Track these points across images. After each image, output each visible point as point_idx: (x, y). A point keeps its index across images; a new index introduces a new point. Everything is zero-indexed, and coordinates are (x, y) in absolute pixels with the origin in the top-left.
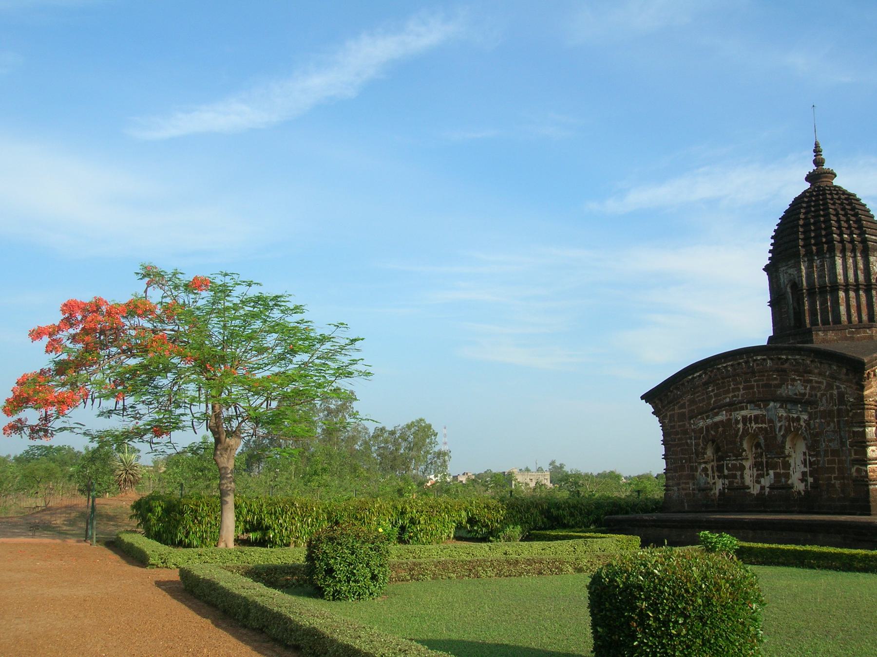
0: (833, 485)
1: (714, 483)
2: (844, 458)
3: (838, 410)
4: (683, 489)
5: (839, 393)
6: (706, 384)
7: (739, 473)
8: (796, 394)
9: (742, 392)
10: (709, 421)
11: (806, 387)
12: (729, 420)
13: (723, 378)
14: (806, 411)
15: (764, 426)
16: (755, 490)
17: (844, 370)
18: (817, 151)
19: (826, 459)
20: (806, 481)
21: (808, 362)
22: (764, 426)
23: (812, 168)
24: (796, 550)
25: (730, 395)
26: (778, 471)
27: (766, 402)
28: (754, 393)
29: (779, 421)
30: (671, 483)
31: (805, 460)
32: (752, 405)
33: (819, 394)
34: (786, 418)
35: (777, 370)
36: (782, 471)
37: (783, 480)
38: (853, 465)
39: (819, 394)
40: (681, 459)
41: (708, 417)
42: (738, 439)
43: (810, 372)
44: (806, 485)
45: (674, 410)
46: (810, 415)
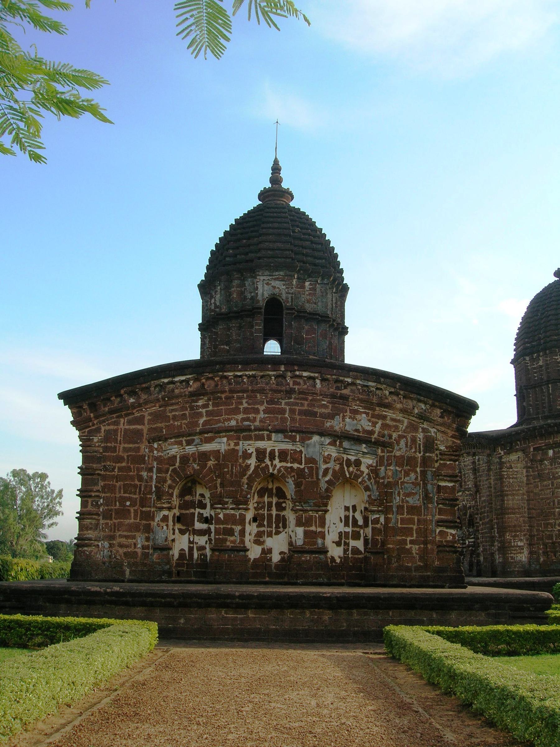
0: (409, 551)
1: (173, 540)
3: (424, 458)
4: (121, 546)
5: (426, 437)
6: (196, 395)
7: (237, 528)
8: (357, 430)
9: (262, 415)
10: (191, 449)
11: (374, 424)
12: (232, 454)
13: (232, 391)
15: (296, 466)
16: (255, 552)
17: (438, 412)
18: (276, 169)
19: (399, 517)
20: (347, 544)
21: (387, 393)
22: (296, 466)
23: (268, 185)
25: (240, 417)
26: (313, 528)
27: (306, 434)
28: (284, 420)
29: (325, 462)
30: (90, 534)
31: (347, 518)
32: (280, 436)
33: (395, 435)
34: (337, 460)
35: (333, 396)
36: (319, 529)
37: (320, 541)
39: (395, 435)
40: (122, 500)
41: (189, 443)
42: (245, 480)
43: (388, 406)
44: (345, 551)
45: (117, 423)
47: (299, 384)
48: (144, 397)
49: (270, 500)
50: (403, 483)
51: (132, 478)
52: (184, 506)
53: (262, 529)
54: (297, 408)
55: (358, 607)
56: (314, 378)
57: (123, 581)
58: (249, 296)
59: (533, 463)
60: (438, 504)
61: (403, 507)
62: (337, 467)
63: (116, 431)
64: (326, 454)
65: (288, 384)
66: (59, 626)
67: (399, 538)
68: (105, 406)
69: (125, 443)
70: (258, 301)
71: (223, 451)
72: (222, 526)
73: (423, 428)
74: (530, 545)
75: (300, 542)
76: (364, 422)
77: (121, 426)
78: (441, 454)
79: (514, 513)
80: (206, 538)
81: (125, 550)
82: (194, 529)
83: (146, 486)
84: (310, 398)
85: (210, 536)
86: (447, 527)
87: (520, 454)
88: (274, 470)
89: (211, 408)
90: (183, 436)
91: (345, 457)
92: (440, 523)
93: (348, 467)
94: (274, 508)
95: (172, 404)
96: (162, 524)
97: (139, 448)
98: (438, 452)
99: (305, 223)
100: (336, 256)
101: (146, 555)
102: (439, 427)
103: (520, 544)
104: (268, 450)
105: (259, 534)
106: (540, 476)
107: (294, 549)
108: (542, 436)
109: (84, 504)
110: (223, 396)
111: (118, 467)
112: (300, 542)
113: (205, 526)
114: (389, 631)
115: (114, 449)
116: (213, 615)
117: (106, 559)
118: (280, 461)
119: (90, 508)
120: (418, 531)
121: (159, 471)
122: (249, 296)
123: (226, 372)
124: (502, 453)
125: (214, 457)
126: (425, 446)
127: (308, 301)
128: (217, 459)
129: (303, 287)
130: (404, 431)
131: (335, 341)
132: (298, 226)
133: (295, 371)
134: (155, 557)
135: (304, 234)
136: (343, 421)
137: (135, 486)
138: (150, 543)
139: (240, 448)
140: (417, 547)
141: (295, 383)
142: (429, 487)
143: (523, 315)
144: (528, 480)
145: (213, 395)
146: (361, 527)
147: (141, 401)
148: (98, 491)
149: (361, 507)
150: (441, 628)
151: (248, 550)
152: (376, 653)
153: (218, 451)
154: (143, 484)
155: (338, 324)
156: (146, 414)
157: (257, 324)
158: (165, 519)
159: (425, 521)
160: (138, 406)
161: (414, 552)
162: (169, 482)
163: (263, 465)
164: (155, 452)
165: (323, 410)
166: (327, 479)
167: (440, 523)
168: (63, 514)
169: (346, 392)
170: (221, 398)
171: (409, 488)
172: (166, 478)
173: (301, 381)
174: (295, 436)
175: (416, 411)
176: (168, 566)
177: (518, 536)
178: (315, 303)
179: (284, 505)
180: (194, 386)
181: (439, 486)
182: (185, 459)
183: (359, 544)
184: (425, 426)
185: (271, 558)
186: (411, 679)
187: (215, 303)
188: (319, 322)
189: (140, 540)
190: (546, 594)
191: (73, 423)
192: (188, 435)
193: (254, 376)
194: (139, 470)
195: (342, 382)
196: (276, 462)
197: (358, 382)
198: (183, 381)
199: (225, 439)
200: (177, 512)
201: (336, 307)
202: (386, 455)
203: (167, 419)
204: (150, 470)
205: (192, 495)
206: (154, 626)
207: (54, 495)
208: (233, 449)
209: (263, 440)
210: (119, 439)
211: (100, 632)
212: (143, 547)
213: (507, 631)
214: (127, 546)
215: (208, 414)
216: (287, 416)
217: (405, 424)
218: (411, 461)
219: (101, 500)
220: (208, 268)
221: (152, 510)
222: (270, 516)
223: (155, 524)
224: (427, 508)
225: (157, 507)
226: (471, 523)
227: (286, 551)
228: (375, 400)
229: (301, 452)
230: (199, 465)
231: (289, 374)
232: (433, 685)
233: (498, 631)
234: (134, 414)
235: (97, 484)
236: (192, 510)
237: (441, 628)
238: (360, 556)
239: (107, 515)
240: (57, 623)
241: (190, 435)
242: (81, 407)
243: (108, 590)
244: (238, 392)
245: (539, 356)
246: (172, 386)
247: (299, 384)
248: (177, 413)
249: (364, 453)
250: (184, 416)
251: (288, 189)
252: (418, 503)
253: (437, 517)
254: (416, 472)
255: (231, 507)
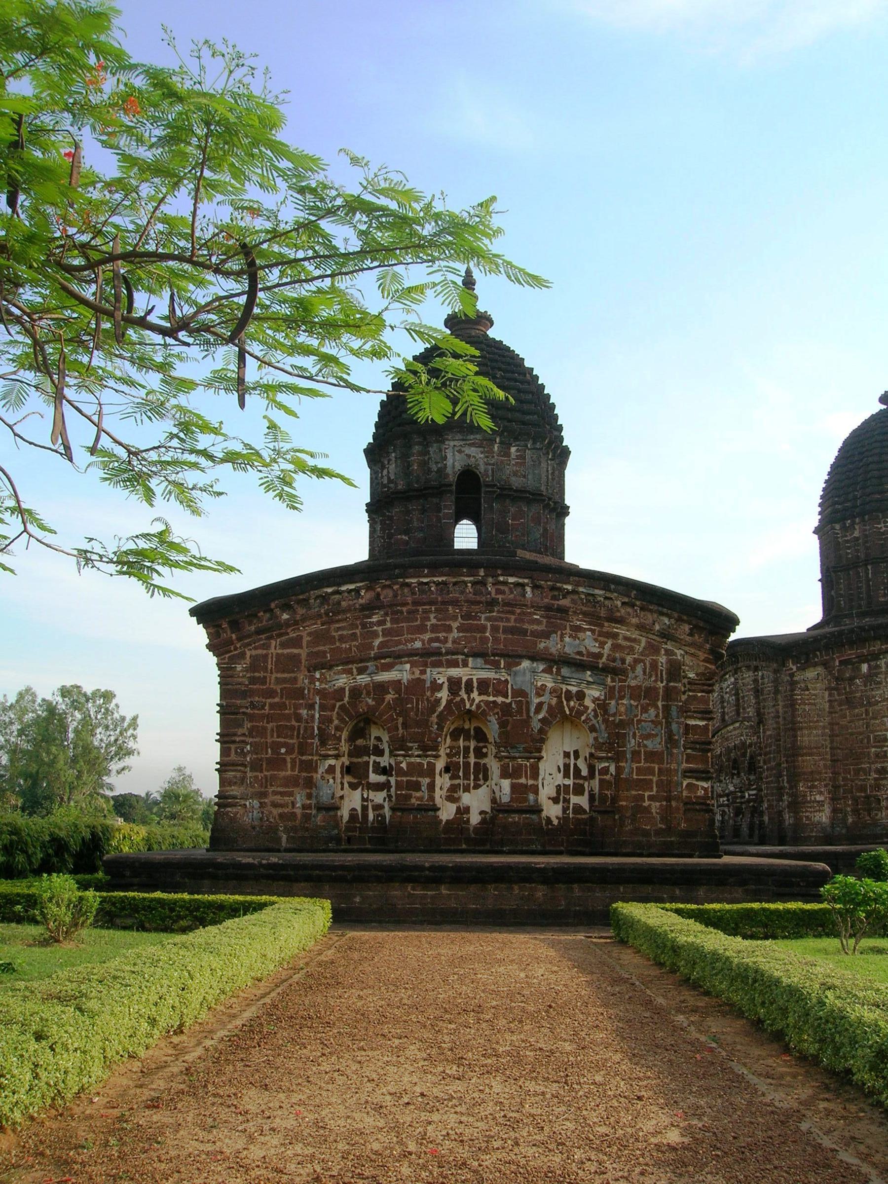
0: (647, 810)
1: (342, 797)
2: (673, 766)
3: (666, 688)
4: (275, 805)
5: (669, 662)
6: (369, 608)
8: (579, 653)
10: (363, 679)
11: (602, 645)
12: (417, 685)
13: (416, 603)
14: (604, 684)
15: (500, 699)
16: (448, 811)
17: (686, 628)
19: (634, 766)
20: (567, 801)
21: (619, 603)
22: (500, 699)
24: (803, 911)
25: (427, 636)
26: (523, 781)
27: (513, 658)
28: (484, 640)
29: (539, 695)
30: (235, 790)
31: (567, 766)
32: (480, 661)
33: (629, 659)
34: (553, 691)
35: (548, 608)
36: (530, 782)
37: (531, 797)
38: (685, 777)
39: (629, 659)
40: (276, 746)
41: (361, 671)
42: (434, 718)
43: (621, 621)
44: (565, 810)
45: (267, 647)
46: (611, 693)
47: (503, 593)
48: (301, 611)
49: (467, 743)
50: (639, 721)
51: (288, 718)
52: (356, 752)
53: (456, 782)
54: (501, 624)
55: (580, 880)
56: (523, 585)
57: (279, 851)
58: (434, 468)
59: (839, 682)
60: (685, 749)
61: (639, 752)
62: (554, 701)
63: (266, 655)
64: (539, 684)
65: (490, 593)
66: (210, 905)
67: (634, 793)
68: (250, 625)
69: (277, 672)
70: (447, 475)
71: (405, 681)
72: (405, 779)
73: (666, 650)
74: (833, 799)
75: (506, 799)
76: (589, 642)
77: (272, 650)
78: (689, 683)
79: (811, 755)
80: (384, 794)
81: (280, 810)
82: (368, 783)
83: (306, 728)
84: (518, 611)
85: (389, 791)
86: (698, 779)
87: (820, 670)
88: (471, 705)
89: (388, 625)
90: (353, 662)
91: (564, 687)
92: (687, 773)
93: (568, 700)
94: (472, 754)
95: (338, 621)
96: (327, 776)
97: (296, 679)
98: (685, 681)
99: (509, 364)
100: (553, 407)
101: (307, 817)
102: (687, 648)
103: (818, 798)
104: (464, 680)
105: (453, 789)
106: (849, 702)
107: (498, 807)
108: (852, 644)
109: (224, 752)
110: (405, 609)
111: (270, 704)
112: (506, 799)
113: (382, 779)
114: (616, 909)
115: (263, 681)
116: (397, 893)
117: (256, 823)
118: (480, 694)
119: (233, 757)
120: (660, 784)
121: (323, 708)
122: (434, 468)
123: (407, 578)
124: (795, 669)
125: (393, 689)
126: (669, 673)
127: (515, 474)
128: (398, 691)
129: (508, 455)
130: (642, 654)
131: (551, 527)
132: (500, 369)
133: (499, 575)
134: (319, 819)
135: (509, 379)
136: (561, 641)
137: (292, 728)
138: (313, 802)
139: (427, 677)
140: (658, 804)
141: (499, 592)
142: (674, 726)
143: (832, 460)
144: (831, 707)
145: (392, 608)
146: (585, 778)
147: (298, 617)
148: (244, 735)
149: (585, 752)
150: (681, 906)
151: (439, 809)
152: (599, 937)
153: (399, 681)
154: (303, 725)
155: (555, 503)
156: (304, 634)
157: (446, 507)
158: (331, 770)
159: (669, 771)
160: (294, 623)
161: (653, 811)
162: (336, 722)
163: (458, 699)
164: (317, 684)
165: (535, 627)
166: (540, 716)
167: (687, 773)
168: (139, 753)
169: (565, 602)
170: (402, 612)
171: (648, 727)
172: (331, 716)
173: (506, 589)
174: (499, 662)
175: (657, 627)
176: (336, 831)
177: (815, 787)
178: (524, 477)
179: (484, 750)
180: (366, 596)
181: (687, 725)
182: (356, 692)
183: (583, 801)
184: (669, 647)
185: (468, 819)
186: (637, 960)
187: (389, 478)
188: (529, 502)
189: (300, 799)
190: (821, 866)
191: (209, 647)
192: (357, 662)
193: (444, 583)
194: (297, 707)
195: (559, 589)
196: (475, 694)
197: (581, 589)
198: (351, 590)
199: (408, 666)
200: (346, 760)
201: (553, 479)
202: (617, 684)
203: (332, 640)
204: (311, 707)
205: (365, 738)
206: (327, 904)
207: (126, 724)
208: (419, 678)
209: (458, 667)
210: (269, 667)
211: (268, 910)
212: (304, 807)
213: (764, 909)
214: (281, 806)
215: (386, 633)
216: (487, 634)
217: (643, 644)
218: (650, 693)
219: (248, 747)
220: (377, 425)
221: (315, 758)
222: (467, 765)
223: (319, 776)
224: (671, 754)
225: (320, 755)
226: (752, 767)
227: (489, 810)
228: (603, 613)
229: (507, 681)
230: (374, 699)
231: (490, 580)
232: (661, 965)
233: (752, 909)
234: (288, 634)
235: (241, 726)
236: (366, 758)
237: (681, 906)
238: (583, 817)
239: (256, 766)
240: (209, 902)
241: (362, 661)
242: (220, 626)
243: (264, 862)
244: (424, 604)
245: (853, 523)
246: (337, 596)
247: (503, 593)
248: (345, 633)
249: (589, 683)
250: (354, 637)
251: (486, 312)
252: (659, 748)
253: (685, 765)
254: (657, 707)
255: (416, 753)
